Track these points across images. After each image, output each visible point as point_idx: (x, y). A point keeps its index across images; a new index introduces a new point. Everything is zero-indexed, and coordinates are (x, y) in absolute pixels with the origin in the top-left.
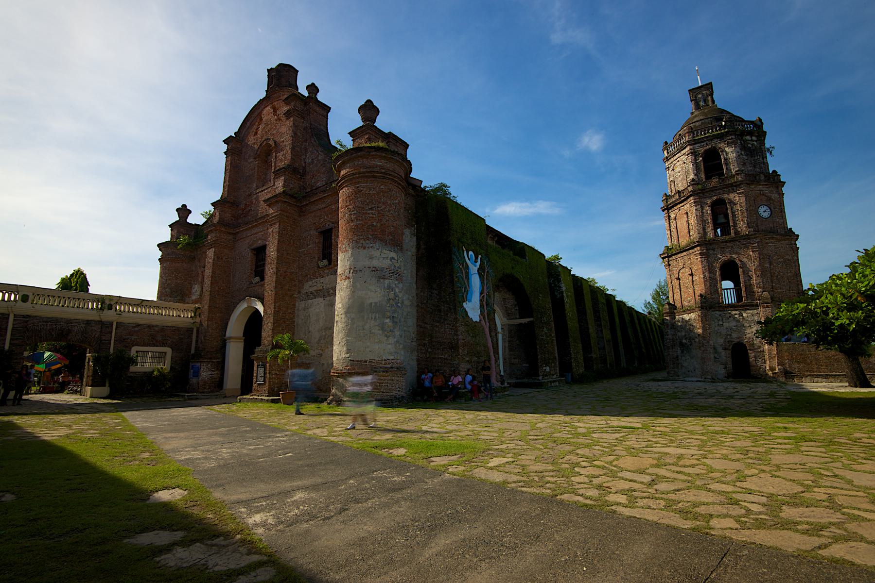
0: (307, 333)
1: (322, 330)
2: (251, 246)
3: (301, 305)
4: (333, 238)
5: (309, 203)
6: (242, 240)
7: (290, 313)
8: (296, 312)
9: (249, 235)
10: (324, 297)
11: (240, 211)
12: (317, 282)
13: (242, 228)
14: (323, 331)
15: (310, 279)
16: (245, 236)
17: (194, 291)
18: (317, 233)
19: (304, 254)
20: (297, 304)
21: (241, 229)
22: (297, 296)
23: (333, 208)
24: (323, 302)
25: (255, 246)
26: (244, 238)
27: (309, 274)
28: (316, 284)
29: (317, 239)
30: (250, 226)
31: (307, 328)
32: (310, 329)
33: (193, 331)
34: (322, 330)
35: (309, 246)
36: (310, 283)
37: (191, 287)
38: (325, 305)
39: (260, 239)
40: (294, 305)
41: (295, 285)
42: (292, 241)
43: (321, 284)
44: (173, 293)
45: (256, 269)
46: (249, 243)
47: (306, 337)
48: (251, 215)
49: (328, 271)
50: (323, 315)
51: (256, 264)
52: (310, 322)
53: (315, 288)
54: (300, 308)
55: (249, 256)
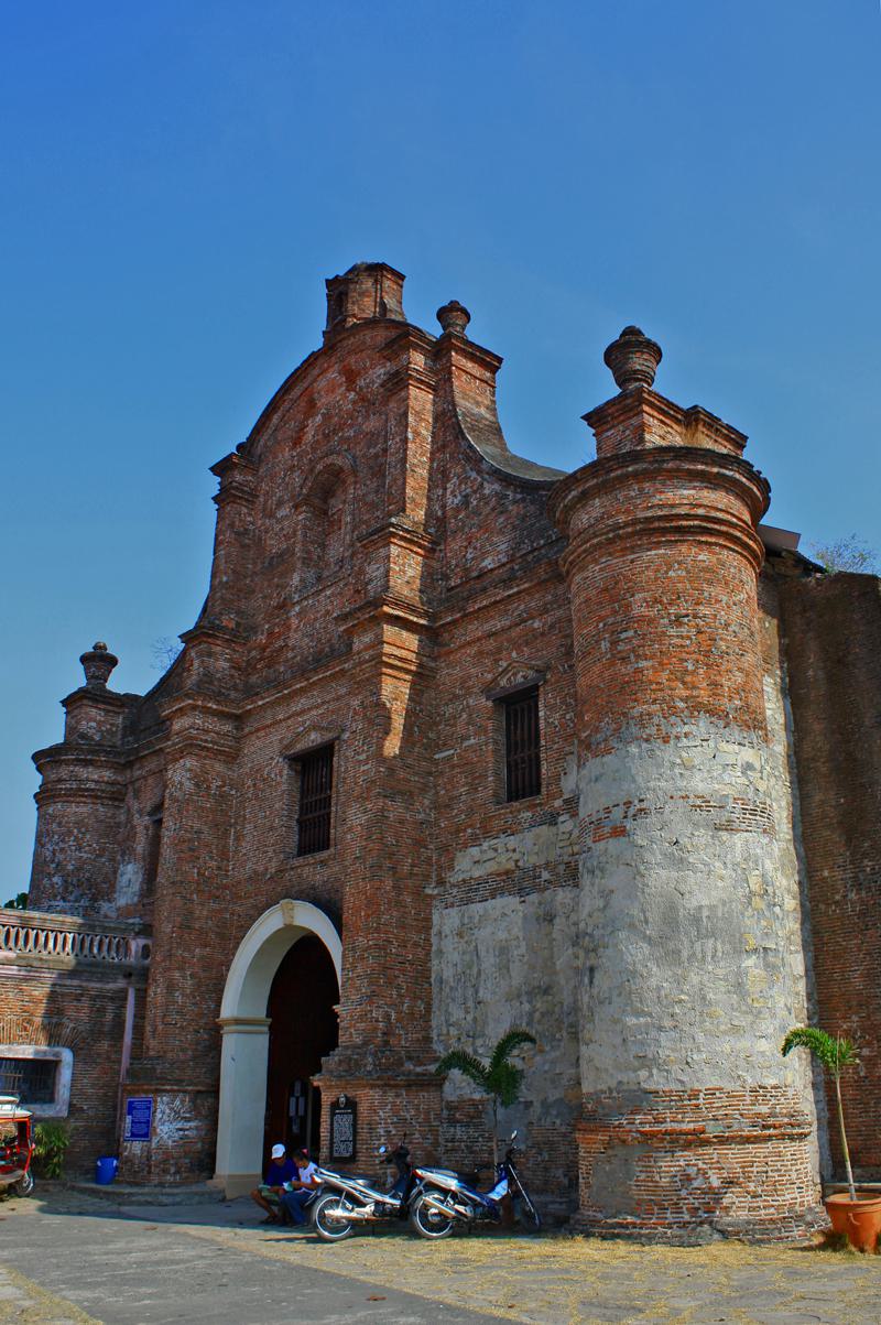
0: (470, 1004)
1: (519, 996)
2: (287, 747)
3: (446, 920)
4: (541, 714)
5: (466, 615)
6: (262, 733)
7: (416, 945)
8: (434, 940)
9: (281, 717)
10: (522, 892)
11: (254, 653)
12: (496, 850)
13: (263, 698)
14: (524, 999)
15: (475, 840)
16: (269, 722)
17: (123, 881)
18: (490, 704)
19: (453, 767)
20: (435, 918)
21: (260, 703)
22: (436, 892)
23: (536, 625)
24: (520, 907)
25: (299, 747)
26: (268, 726)
27: (470, 826)
28: (493, 854)
29: (489, 719)
30: (286, 692)
31: (470, 992)
32: (481, 994)
33: (125, 999)
34: (519, 996)
35: (466, 743)
36: (475, 851)
37: (115, 872)
38: (525, 917)
39: (315, 727)
40: (428, 919)
41: (430, 858)
42: (416, 729)
43: (511, 854)
44: (70, 888)
45: (300, 815)
46: (281, 741)
47: (470, 1018)
49: (530, 814)
50: (523, 950)
51: (302, 798)
53: (491, 867)
54: (446, 930)
55: (282, 777)
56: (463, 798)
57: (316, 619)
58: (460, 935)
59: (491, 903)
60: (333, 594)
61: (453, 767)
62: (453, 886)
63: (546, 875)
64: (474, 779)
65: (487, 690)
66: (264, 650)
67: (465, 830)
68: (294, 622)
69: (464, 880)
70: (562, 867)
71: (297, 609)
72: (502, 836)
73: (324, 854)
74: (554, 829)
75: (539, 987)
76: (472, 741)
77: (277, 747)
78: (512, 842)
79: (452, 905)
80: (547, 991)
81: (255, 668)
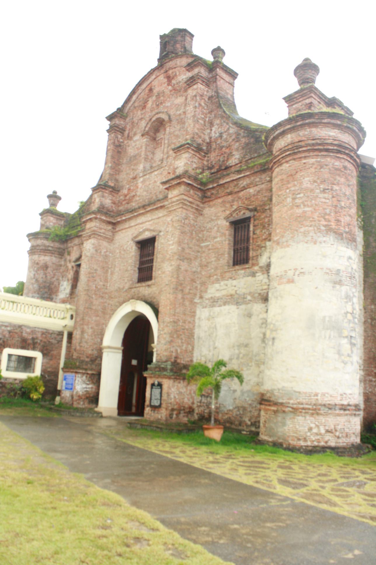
2: (135, 237)
5: (218, 185)
10: (237, 303)
12: (227, 285)
15: (217, 281)
19: (209, 250)
32: (216, 345)
36: (217, 286)
48: (136, 201)
52: (216, 336)
53: (224, 293)
54: (203, 317)
56: (213, 263)
57: (150, 184)
58: (208, 319)
59: (223, 308)
60: (158, 174)
61: (209, 250)
62: (207, 299)
63: (249, 298)
64: (219, 255)
65: (226, 218)
66: (126, 196)
67: (213, 276)
68: (140, 185)
69: (212, 298)
70: (257, 295)
71: (141, 179)
72: (230, 280)
73: (149, 283)
74: (254, 279)
75: (243, 344)
76: (218, 239)
77: (131, 237)
78: (234, 282)
79: (206, 307)
80: (246, 346)
81: (121, 204)
